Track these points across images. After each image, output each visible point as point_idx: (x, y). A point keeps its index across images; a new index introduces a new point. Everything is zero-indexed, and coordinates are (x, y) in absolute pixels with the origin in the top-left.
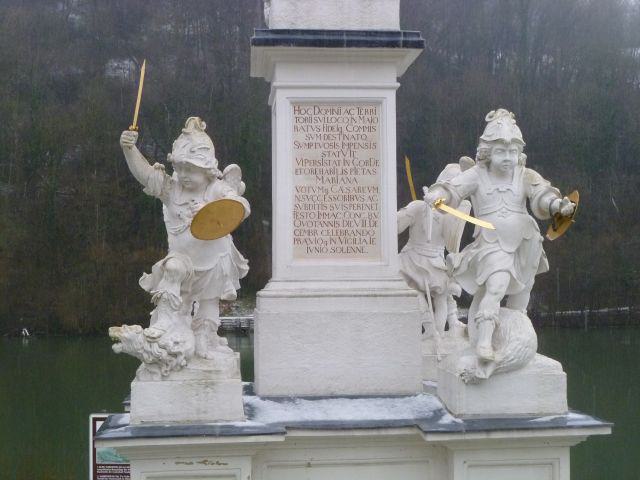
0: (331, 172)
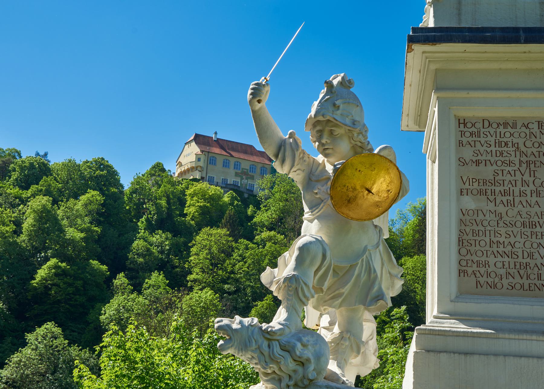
0: (504, 193)
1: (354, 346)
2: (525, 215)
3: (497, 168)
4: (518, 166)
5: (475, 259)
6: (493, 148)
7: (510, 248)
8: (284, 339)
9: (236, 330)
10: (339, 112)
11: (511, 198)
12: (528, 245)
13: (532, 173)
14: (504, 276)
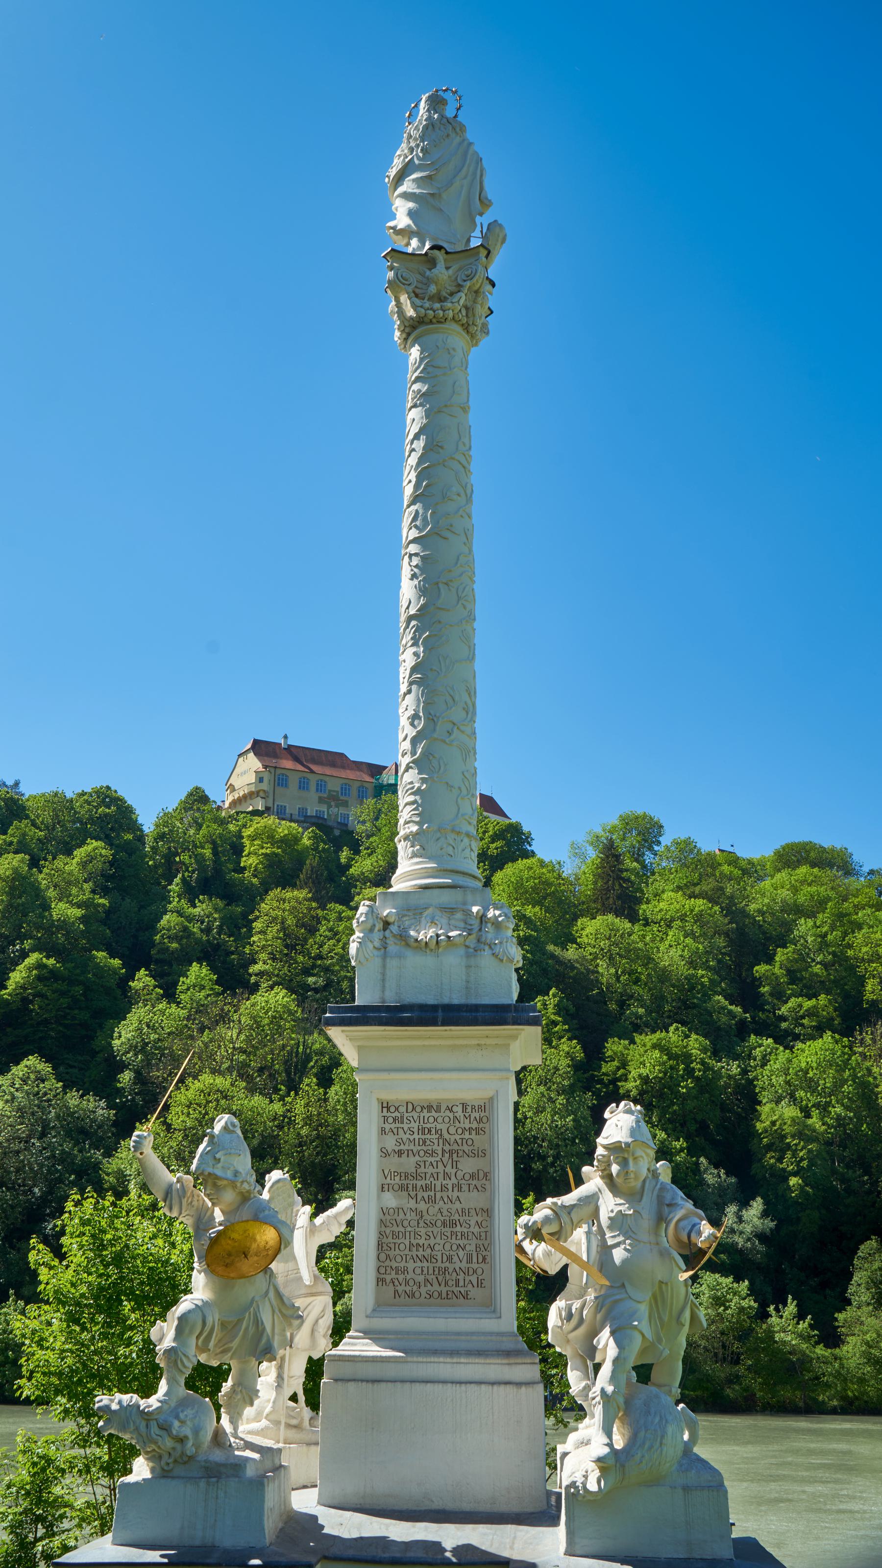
0: (426, 1188)
1: (247, 1399)
2: (445, 1213)
3: (419, 1159)
4: (440, 1156)
5: (394, 1264)
6: (416, 1136)
7: (429, 1251)
8: (161, 1418)
9: (115, 1411)
10: (220, 1165)
11: (432, 1194)
12: (447, 1247)
13: (454, 1163)
14: (422, 1284)
